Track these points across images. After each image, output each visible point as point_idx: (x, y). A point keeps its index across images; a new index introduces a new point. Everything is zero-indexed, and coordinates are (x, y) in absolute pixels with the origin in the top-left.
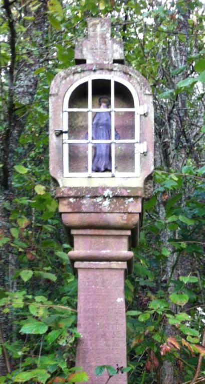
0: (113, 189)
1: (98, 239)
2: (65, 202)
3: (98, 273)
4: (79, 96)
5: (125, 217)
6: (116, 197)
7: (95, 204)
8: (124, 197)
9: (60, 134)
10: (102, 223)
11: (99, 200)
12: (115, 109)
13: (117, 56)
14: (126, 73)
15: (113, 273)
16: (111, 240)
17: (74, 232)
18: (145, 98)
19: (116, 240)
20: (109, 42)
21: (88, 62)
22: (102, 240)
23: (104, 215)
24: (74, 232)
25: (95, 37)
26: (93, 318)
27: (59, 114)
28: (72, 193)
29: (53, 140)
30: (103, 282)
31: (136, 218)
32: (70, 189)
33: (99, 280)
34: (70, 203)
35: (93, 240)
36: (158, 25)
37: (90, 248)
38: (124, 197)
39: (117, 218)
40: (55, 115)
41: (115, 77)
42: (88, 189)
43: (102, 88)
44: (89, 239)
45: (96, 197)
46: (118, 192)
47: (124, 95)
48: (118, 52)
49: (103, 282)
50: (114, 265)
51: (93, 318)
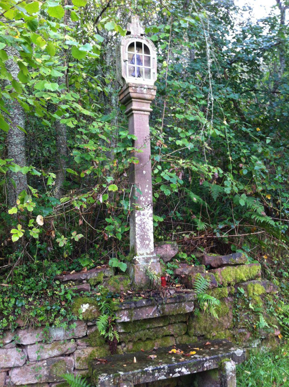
0: (147, 85)
1: (141, 103)
2: (131, 88)
3: (140, 115)
4: (131, 46)
5: (151, 96)
6: (148, 88)
7: (141, 90)
8: (151, 89)
9: (125, 61)
10: (143, 98)
11: (142, 89)
12: (143, 54)
13: (142, 33)
14: (147, 41)
15: (145, 116)
16: (145, 104)
17: (133, 100)
18: (154, 51)
19: (146, 104)
20: (139, 26)
21: (132, 33)
22: (142, 104)
23: (144, 95)
24: (133, 100)
25: (134, 23)
26: (140, 132)
27: (125, 53)
28: (134, 85)
29: (123, 63)
30: (142, 119)
31: (154, 97)
32: (133, 84)
33: (141, 118)
34: (133, 89)
35: (139, 103)
36: (247, 81)
37: (138, 106)
38: (151, 89)
39: (148, 96)
40: (123, 53)
41: (144, 42)
42: (139, 85)
43: (139, 45)
44: (138, 103)
45: (141, 88)
46: (149, 87)
47: (147, 50)
48: (142, 31)
49: (142, 119)
50: (146, 113)
51: (140, 132)
